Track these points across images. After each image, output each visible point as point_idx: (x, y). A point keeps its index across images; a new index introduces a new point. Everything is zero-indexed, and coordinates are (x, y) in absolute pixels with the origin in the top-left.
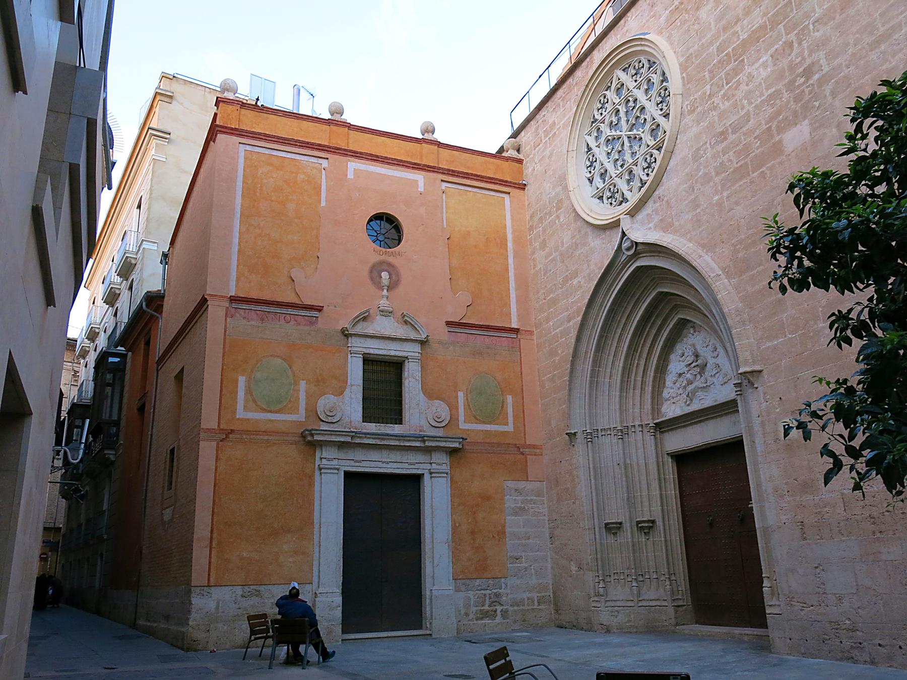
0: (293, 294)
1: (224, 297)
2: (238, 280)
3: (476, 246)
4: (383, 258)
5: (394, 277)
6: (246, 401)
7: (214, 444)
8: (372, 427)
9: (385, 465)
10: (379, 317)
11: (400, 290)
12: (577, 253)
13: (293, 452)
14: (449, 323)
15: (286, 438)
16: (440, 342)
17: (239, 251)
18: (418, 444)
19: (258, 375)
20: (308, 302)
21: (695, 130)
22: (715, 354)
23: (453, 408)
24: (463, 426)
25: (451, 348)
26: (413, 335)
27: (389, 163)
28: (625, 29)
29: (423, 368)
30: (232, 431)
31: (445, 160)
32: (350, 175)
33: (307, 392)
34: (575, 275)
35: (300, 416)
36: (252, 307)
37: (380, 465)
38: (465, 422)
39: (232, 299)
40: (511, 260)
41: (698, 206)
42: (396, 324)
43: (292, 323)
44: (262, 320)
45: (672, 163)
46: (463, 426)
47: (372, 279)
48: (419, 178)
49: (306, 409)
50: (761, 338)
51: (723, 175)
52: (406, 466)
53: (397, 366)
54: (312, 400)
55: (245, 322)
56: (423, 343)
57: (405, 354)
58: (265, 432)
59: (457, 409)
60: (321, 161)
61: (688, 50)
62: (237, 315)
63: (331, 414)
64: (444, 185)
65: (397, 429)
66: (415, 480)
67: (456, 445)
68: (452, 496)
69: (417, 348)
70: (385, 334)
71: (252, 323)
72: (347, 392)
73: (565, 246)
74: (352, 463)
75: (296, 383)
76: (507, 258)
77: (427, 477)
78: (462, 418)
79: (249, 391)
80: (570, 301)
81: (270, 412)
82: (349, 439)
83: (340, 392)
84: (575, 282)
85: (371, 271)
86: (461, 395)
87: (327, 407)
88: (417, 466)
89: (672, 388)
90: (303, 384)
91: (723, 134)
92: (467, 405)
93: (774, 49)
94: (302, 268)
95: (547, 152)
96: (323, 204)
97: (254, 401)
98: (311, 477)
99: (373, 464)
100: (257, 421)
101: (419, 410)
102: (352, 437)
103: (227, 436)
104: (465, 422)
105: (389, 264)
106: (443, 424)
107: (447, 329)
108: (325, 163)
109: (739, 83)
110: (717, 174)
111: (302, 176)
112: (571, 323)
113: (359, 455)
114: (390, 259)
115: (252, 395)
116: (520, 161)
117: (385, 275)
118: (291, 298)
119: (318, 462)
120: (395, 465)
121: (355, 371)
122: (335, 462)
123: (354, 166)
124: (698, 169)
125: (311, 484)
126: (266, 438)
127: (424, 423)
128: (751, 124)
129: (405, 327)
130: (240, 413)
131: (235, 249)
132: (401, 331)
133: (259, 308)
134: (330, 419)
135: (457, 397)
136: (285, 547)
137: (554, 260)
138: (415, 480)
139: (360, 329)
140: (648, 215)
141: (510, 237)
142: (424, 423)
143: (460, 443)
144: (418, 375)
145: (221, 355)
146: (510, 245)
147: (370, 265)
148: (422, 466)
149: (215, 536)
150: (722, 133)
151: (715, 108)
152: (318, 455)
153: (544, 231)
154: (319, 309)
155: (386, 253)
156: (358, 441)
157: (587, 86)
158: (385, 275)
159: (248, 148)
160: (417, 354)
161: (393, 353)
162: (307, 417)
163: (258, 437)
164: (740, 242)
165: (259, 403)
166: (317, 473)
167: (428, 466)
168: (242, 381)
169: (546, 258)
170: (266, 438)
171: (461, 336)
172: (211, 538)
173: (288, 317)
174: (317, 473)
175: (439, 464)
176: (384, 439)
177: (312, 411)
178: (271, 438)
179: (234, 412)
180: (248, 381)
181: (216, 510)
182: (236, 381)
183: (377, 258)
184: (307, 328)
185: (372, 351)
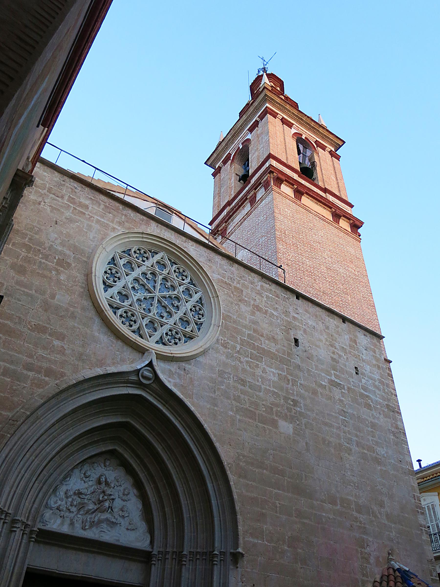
12: (71, 323)
21: (223, 358)
22: (125, 498)
28: (184, 244)
34: (61, 337)
41: (216, 405)
45: (200, 359)
50: (247, 532)
51: (238, 404)
61: (229, 312)
73: (56, 301)
80: (40, 352)
84: (56, 343)
89: (62, 500)
91: (243, 382)
93: (281, 372)
95: (68, 214)
109: (257, 366)
110: (234, 399)
112: (31, 374)
124: (222, 383)
128: (261, 394)
137: (31, 296)
140: (170, 370)
150: (242, 380)
151: (241, 362)
153: (27, 260)
157: (143, 233)
164: (244, 456)
169: (17, 283)
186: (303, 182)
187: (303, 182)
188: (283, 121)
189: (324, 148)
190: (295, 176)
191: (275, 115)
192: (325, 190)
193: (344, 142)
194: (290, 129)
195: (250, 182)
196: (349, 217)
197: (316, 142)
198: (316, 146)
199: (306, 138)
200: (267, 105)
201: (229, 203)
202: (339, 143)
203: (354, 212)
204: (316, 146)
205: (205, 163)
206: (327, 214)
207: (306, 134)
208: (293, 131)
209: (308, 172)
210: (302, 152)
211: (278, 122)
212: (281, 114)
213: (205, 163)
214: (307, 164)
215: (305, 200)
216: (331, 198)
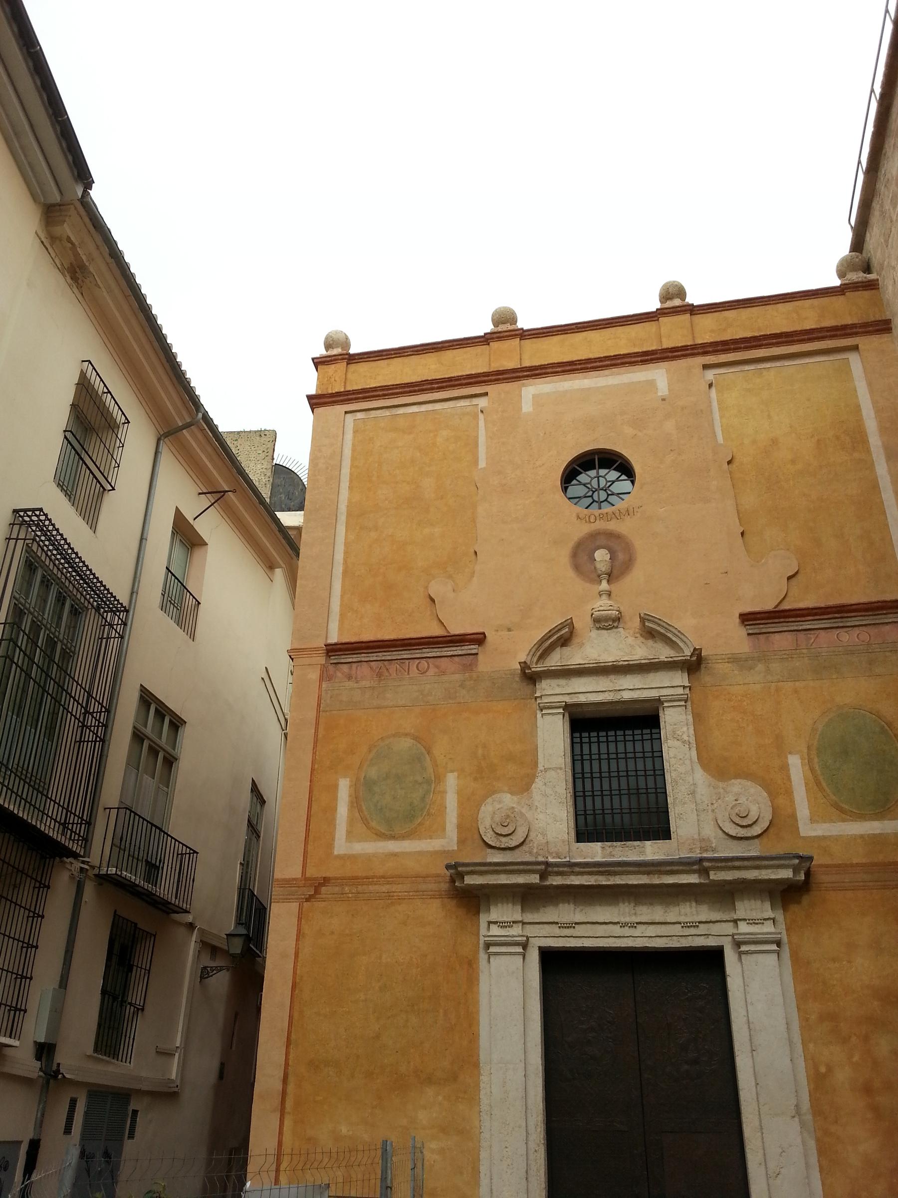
0: (435, 623)
1: (316, 649)
2: (342, 616)
3: (793, 462)
4: (600, 525)
5: (621, 556)
6: (351, 822)
7: (295, 906)
8: (595, 852)
9: (627, 931)
10: (594, 633)
11: (636, 577)
13: (436, 913)
14: (747, 618)
15: (423, 887)
16: (734, 659)
17: (345, 572)
18: (693, 879)
19: (373, 773)
20: (456, 629)
23: (777, 790)
24: (808, 829)
25: (760, 667)
26: (664, 653)
27: (595, 369)
29: (698, 719)
30: (326, 881)
31: (707, 330)
32: (527, 407)
33: (459, 793)
35: (446, 840)
36: (363, 657)
37: (616, 930)
38: (812, 821)
39: (332, 650)
40: (882, 469)
42: (630, 640)
43: (432, 672)
44: (379, 675)
46: (808, 829)
47: (577, 568)
48: (659, 376)
49: (460, 827)
52: (677, 930)
53: (644, 720)
54: (470, 805)
55: (351, 684)
56: (694, 665)
57: (654, 694)
58: (385, 879)
59: (789, 792)
60: (475, 401)
62: (339, 674)
63: (505, 831)
64: (710, 375)
65: (651, 850)
66: (710, 961)
67: (786, 874)
68: (802, 998)
69: (680, 678)
70: (609, 662)
71: (365, 683)
72: (538, 784)
74: (556, 930)
75: (439, 779)
76: (871, 466)
77: (730, 956)
78: (803, 811)
79: (355, 802)
81: (393, 837)
82: (535, 879)
83: (524, 786)
85: (575, 554)
86: (795, 762)
87: (497, 819)
88: (703, 929)
90: (451, 781)
92: (815, 784)
94: (450, 577)
96: (482, 464)
97: (365, 822)
98: (471, 964)
99: (600, 930)
100: (369, 858)
101: (701, 808)
102: (543, 876)
103: (317, 891)
104: (812, 821)
105: (612, 535)
106: (757, 830)
107: (742, 632)
108: (482, 402)
111: (445, 433)
113: (566, 912)
114: (612, 526)
115: (360, 811)
116: (872, 286)
117: (601, 556)
118: (437, 631)
119: (483, 931)
120: (651, 930)
121: (553, 738)
122: (516, 931)
123: (531, 392)
125: (472, 980)
126: (385, 888)
127: (709, 831)
129: (650, 642)
130: (341, 845)
131: (338, 570)
132: (642, 651)
133: (373, 657)
134: (505, 842)
135: (785, 768)
136: (423, 1117)
138: (710, 961)
139: (555, 660)
141: (871, 424)
142: (709, 831)
143: (796, 870)
144: (687, 732)
145: (311, 746)
146: (875, 441)
147: (571, 544)
148: (716, 929)
149: (291, 1088)
152: (483, 919)
154: (479, 639)
155: (601, 517)
156: (556, 881)
158: (601, 556)
159: (359, 415)
160: (680, 691)
161: (627, 696)
162: (461, 842)
163: (371, 888)
165: (373, 824)
166: (483, 956)
167: (729, 928)
168: (344, 788)
170: (385, 888)
171: (781, 640)
172: (284, 1093)
173: (424, 663)
174: (483, 956)
175: (753, 922)
176: (615, 874)
177: (468, 830)
178: (394, 888)
179: (330, 845)
180: (355, 787)
181: (293, 1036)
182: (335, 787)
183: (585, 529)
184: (458, 677)
185: (582, 699)
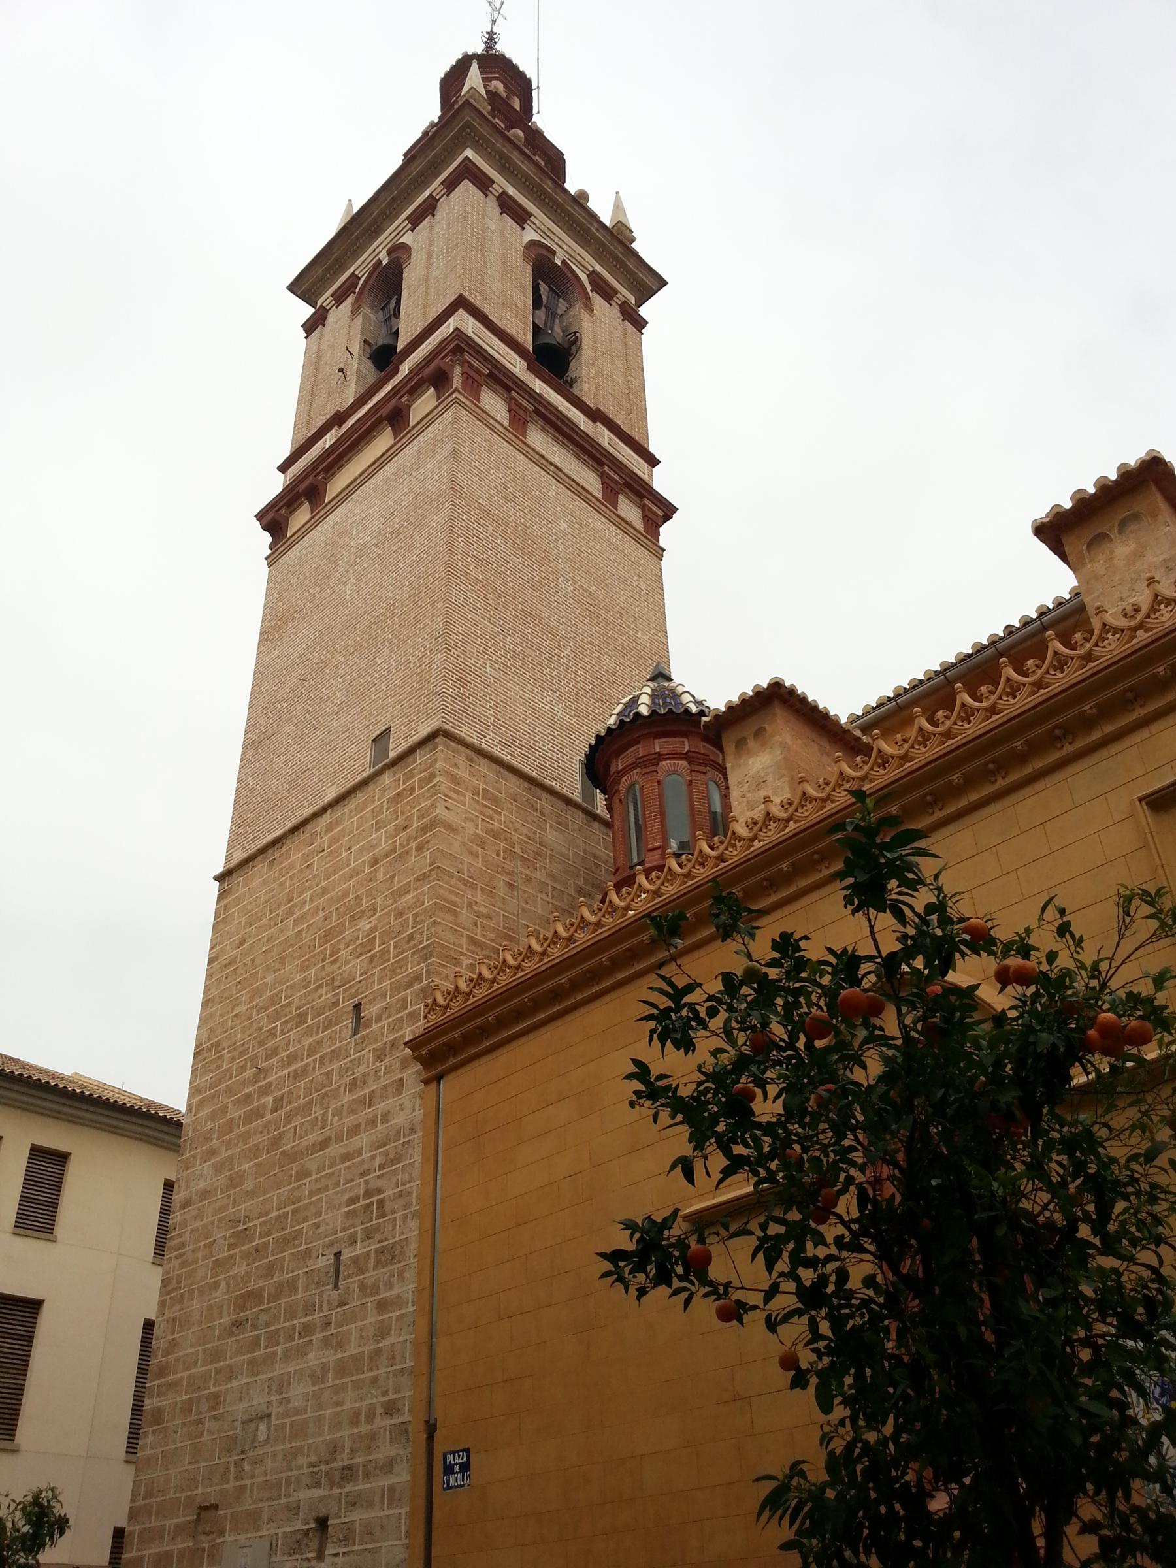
186: (538, 386)
187: (538, 386)
188: (507, 206)
189: (608, 294)
190: (517, 366)
191: (483, 183)
192: (596, 416)
193: (663, 283)
194: (519, 228)
195: (397, 371)
196: (642, 492)
197: (594, 276)
198: (589, 288)
199: (564, 262)
200: (469, 153)
201: (338, 419)
202: (648, 283)
203: (662, 481)
204: (589, 288)
205: (292, 288)
206: (591, 480)
207: (565, 248)
208: (530, 235)
209: (554, 358)
210: (544, 299)
211: (492, 205)
212: (501, 183)
213: (292, 288)
214: (557, 334)
215: (537, 438)
216: (605, 437)
